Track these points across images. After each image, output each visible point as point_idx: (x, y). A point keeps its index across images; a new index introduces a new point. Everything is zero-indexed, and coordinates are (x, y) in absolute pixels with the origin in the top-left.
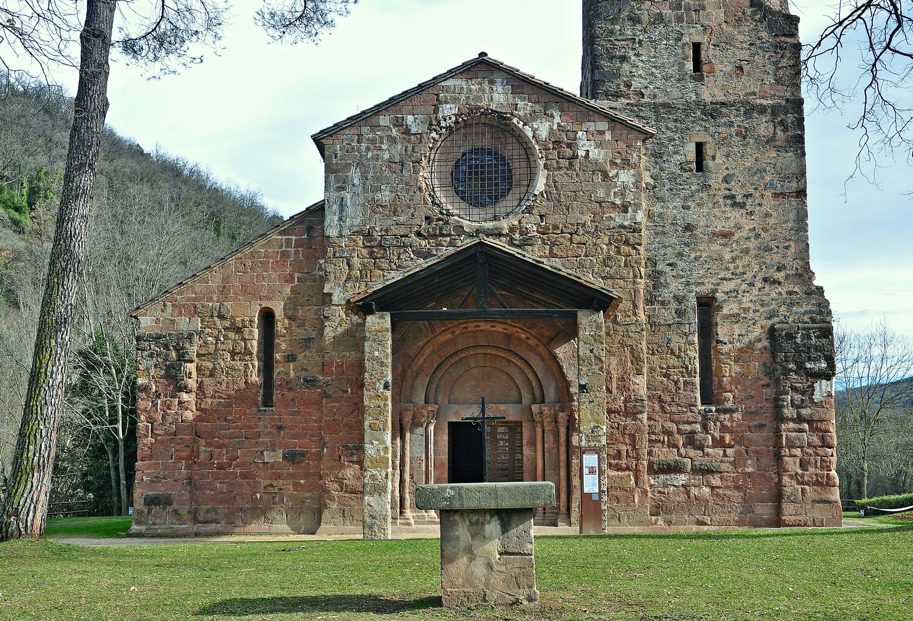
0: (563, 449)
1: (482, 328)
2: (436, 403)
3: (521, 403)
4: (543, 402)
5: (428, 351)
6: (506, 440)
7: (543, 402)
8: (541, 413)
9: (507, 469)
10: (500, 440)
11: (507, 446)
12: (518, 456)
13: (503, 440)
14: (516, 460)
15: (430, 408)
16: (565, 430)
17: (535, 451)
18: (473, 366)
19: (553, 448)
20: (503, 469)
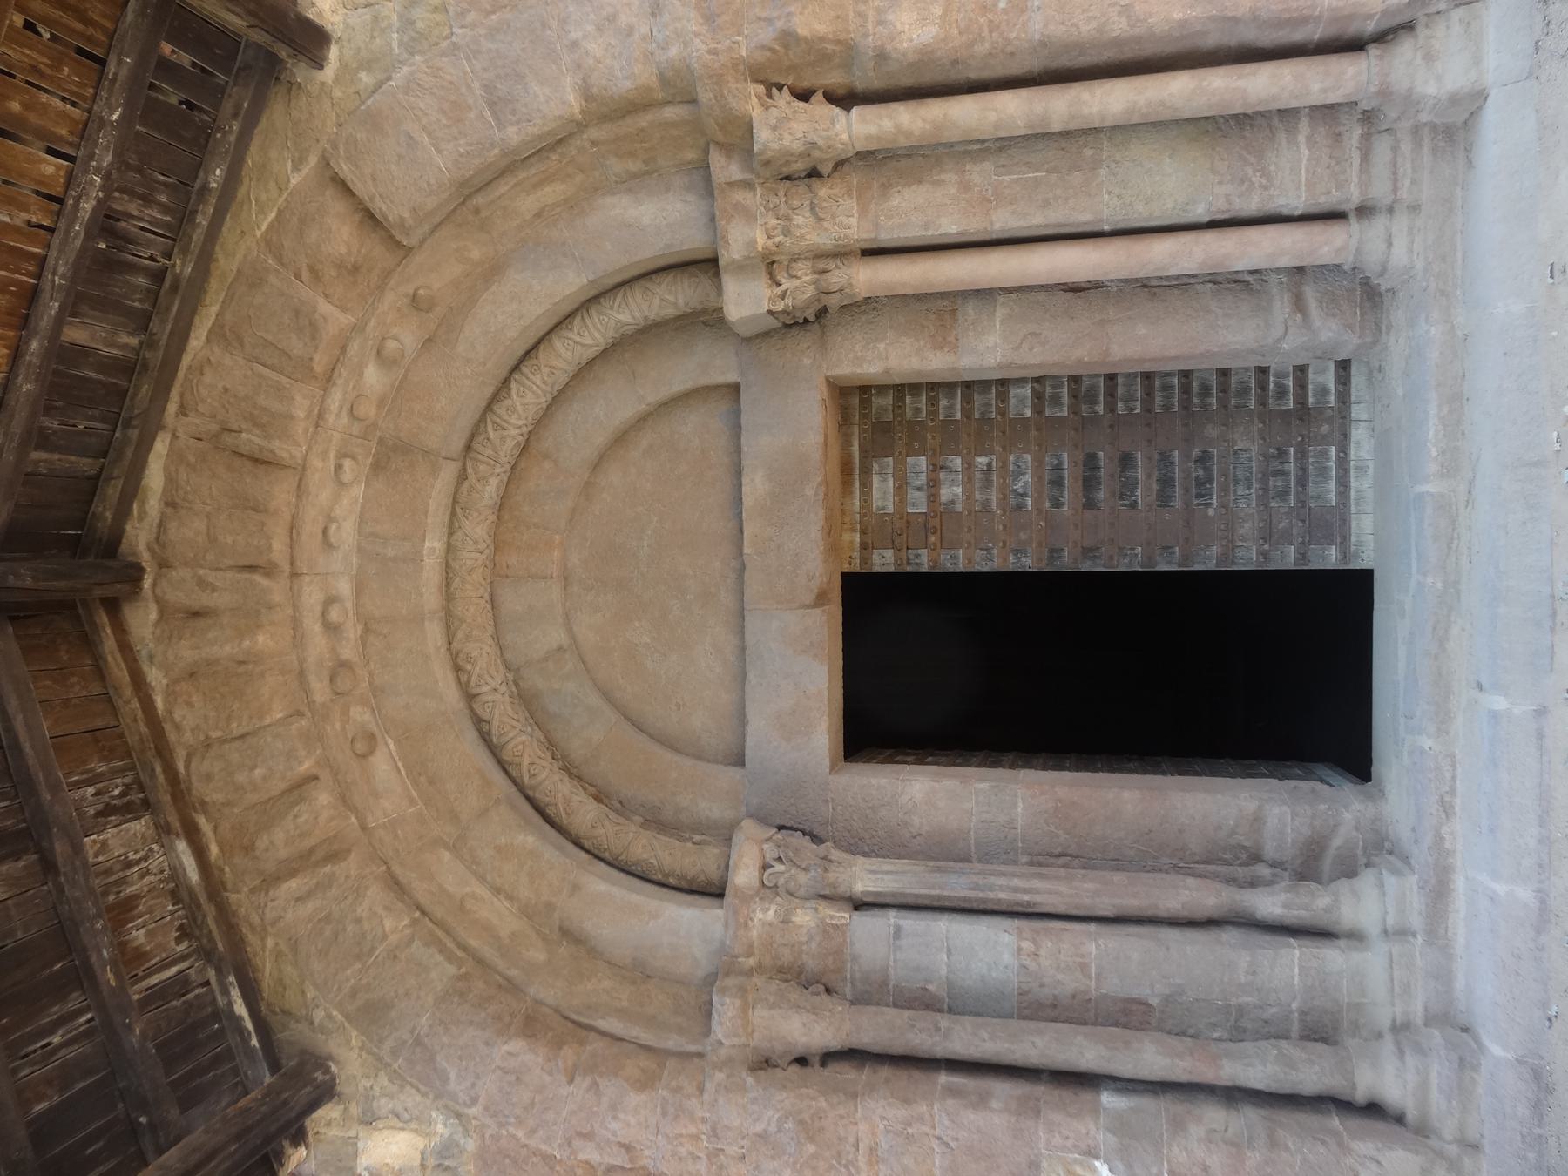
0: (966, 114)
1: (344, 587)
2: (725, 835)
3: (735, 389)
4: (707, 265)
5: (450, 875)
6: (935, 468)
7: (707, 265)
8: (770, 265)
9: (1091, 462)
10: (933, 498)
11: (969, 465)
12: (1020, 401)
13: (934, 484)
14: (1038, 410)
15: (744, 875)
16: (855, 111)
17: (984, 295)
18: (557, 636)
19: (966, 187)
20: (1089, 483)
